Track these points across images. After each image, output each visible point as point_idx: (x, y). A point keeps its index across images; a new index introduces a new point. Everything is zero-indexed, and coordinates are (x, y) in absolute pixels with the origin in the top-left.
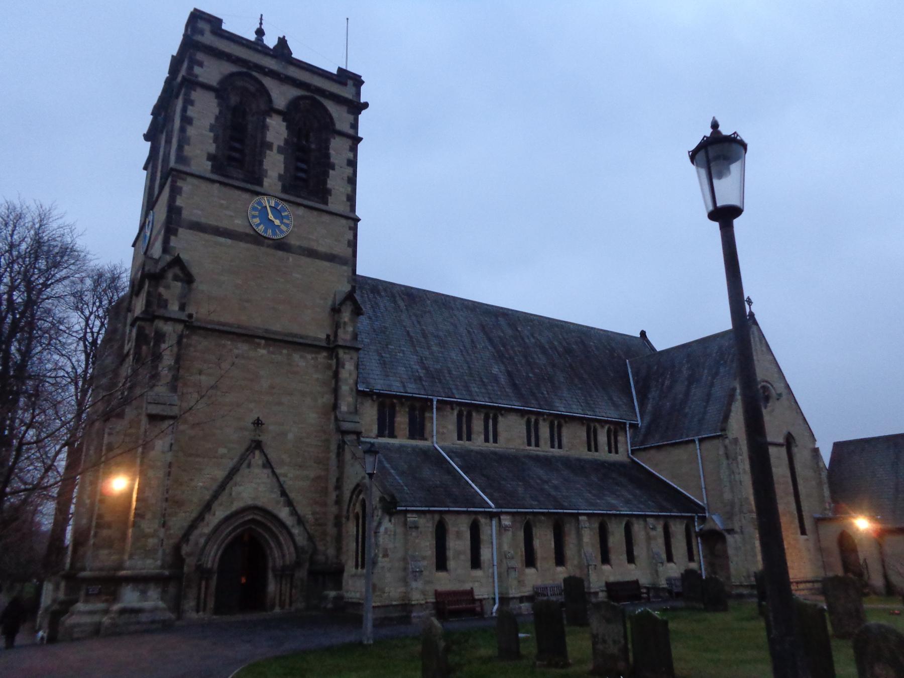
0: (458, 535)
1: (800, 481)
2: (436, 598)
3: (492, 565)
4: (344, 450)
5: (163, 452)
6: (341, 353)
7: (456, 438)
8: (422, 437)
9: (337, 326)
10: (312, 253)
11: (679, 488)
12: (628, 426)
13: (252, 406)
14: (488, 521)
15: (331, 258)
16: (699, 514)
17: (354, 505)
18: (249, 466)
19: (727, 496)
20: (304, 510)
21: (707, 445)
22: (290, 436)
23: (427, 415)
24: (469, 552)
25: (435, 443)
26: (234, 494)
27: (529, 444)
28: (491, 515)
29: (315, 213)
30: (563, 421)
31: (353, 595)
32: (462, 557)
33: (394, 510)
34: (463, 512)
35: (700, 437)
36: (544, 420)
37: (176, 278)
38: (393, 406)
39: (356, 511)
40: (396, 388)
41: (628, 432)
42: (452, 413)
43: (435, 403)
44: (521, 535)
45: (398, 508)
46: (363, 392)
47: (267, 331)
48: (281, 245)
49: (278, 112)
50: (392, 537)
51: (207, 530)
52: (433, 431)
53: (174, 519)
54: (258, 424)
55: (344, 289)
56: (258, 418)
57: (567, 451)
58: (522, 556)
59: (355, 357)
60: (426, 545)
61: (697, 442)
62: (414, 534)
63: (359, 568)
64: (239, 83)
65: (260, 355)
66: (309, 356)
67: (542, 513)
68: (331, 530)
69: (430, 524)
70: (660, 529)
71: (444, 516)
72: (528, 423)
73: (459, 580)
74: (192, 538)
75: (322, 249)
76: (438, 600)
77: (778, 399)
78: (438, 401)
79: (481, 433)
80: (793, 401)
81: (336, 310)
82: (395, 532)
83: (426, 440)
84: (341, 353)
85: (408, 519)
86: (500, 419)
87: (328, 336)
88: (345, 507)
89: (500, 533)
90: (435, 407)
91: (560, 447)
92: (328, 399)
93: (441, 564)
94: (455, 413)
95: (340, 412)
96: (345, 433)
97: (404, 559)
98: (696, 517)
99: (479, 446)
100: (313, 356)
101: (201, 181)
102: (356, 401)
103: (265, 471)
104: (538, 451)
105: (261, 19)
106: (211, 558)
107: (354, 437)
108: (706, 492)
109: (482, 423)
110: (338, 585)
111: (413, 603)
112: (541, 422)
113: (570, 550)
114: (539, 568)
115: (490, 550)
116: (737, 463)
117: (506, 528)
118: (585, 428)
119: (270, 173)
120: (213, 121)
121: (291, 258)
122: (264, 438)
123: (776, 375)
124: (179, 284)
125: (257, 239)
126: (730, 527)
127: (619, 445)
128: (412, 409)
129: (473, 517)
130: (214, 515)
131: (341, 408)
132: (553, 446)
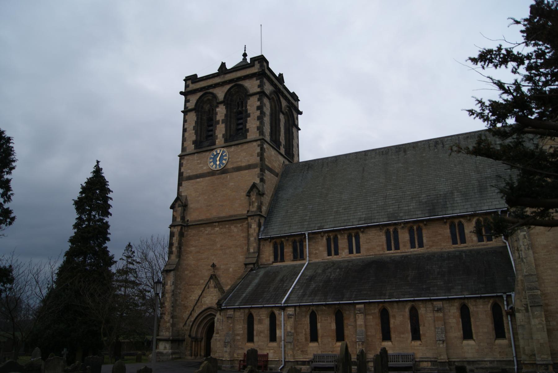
0: (260, 322)
5: (171, 286)
7: (327, 255)
9: (251, 204)
10: (239, 169)
13: (213, 257)
16: (508, 294)
18: (208, 288)
22: (231, 270)
23: (304, 244)
26: (203, 302)
27: (389, 248)
29: (240, 146)
32: (262, 335)
34: (261, 308)
37: (179, 206)
38: (282, 244)
43: (307, 235)
44: (307, 321)
45: (222, 307)
47: (219, 218)
48: (224, 171)
49: (221, 103)
50: (221, 323)
51: (193, 319)
53: (185, 314)
54: (213, 266)
56: (213, 263)
57: (427, 248)
58: (305, 334)
59: (257, 220)
60: (241, 328)
64: (205, 99)
65: (216, 231)
66: (239, 225)
67: (322, 305)
72: (388, 234)
73: (260, 349)
74: (187, 323)
75: (243, 164)
78: (309, 234)
79: (345, 248)
83: (304, 259)
86: (361, 235)
90: (307, 238)
91: (421, 245)
94: (325, 239)
100: (241, 224)
101: (190, 156)
103: (216, 289)
104: (359, 256)
105: (245, 48)
106: (194, 332)
113: (348, 331)
114: (320, 343)
117: (289, 316)
118: (448, 226)
119: (218, 136)
120: (194, 125)
121: (228, 176)
122: (219, 273)
124: (180, 208)
125: (212, 173)
128: (294, 242)
129: (270, 309)
130: (195, 312)
132: (413, 246)
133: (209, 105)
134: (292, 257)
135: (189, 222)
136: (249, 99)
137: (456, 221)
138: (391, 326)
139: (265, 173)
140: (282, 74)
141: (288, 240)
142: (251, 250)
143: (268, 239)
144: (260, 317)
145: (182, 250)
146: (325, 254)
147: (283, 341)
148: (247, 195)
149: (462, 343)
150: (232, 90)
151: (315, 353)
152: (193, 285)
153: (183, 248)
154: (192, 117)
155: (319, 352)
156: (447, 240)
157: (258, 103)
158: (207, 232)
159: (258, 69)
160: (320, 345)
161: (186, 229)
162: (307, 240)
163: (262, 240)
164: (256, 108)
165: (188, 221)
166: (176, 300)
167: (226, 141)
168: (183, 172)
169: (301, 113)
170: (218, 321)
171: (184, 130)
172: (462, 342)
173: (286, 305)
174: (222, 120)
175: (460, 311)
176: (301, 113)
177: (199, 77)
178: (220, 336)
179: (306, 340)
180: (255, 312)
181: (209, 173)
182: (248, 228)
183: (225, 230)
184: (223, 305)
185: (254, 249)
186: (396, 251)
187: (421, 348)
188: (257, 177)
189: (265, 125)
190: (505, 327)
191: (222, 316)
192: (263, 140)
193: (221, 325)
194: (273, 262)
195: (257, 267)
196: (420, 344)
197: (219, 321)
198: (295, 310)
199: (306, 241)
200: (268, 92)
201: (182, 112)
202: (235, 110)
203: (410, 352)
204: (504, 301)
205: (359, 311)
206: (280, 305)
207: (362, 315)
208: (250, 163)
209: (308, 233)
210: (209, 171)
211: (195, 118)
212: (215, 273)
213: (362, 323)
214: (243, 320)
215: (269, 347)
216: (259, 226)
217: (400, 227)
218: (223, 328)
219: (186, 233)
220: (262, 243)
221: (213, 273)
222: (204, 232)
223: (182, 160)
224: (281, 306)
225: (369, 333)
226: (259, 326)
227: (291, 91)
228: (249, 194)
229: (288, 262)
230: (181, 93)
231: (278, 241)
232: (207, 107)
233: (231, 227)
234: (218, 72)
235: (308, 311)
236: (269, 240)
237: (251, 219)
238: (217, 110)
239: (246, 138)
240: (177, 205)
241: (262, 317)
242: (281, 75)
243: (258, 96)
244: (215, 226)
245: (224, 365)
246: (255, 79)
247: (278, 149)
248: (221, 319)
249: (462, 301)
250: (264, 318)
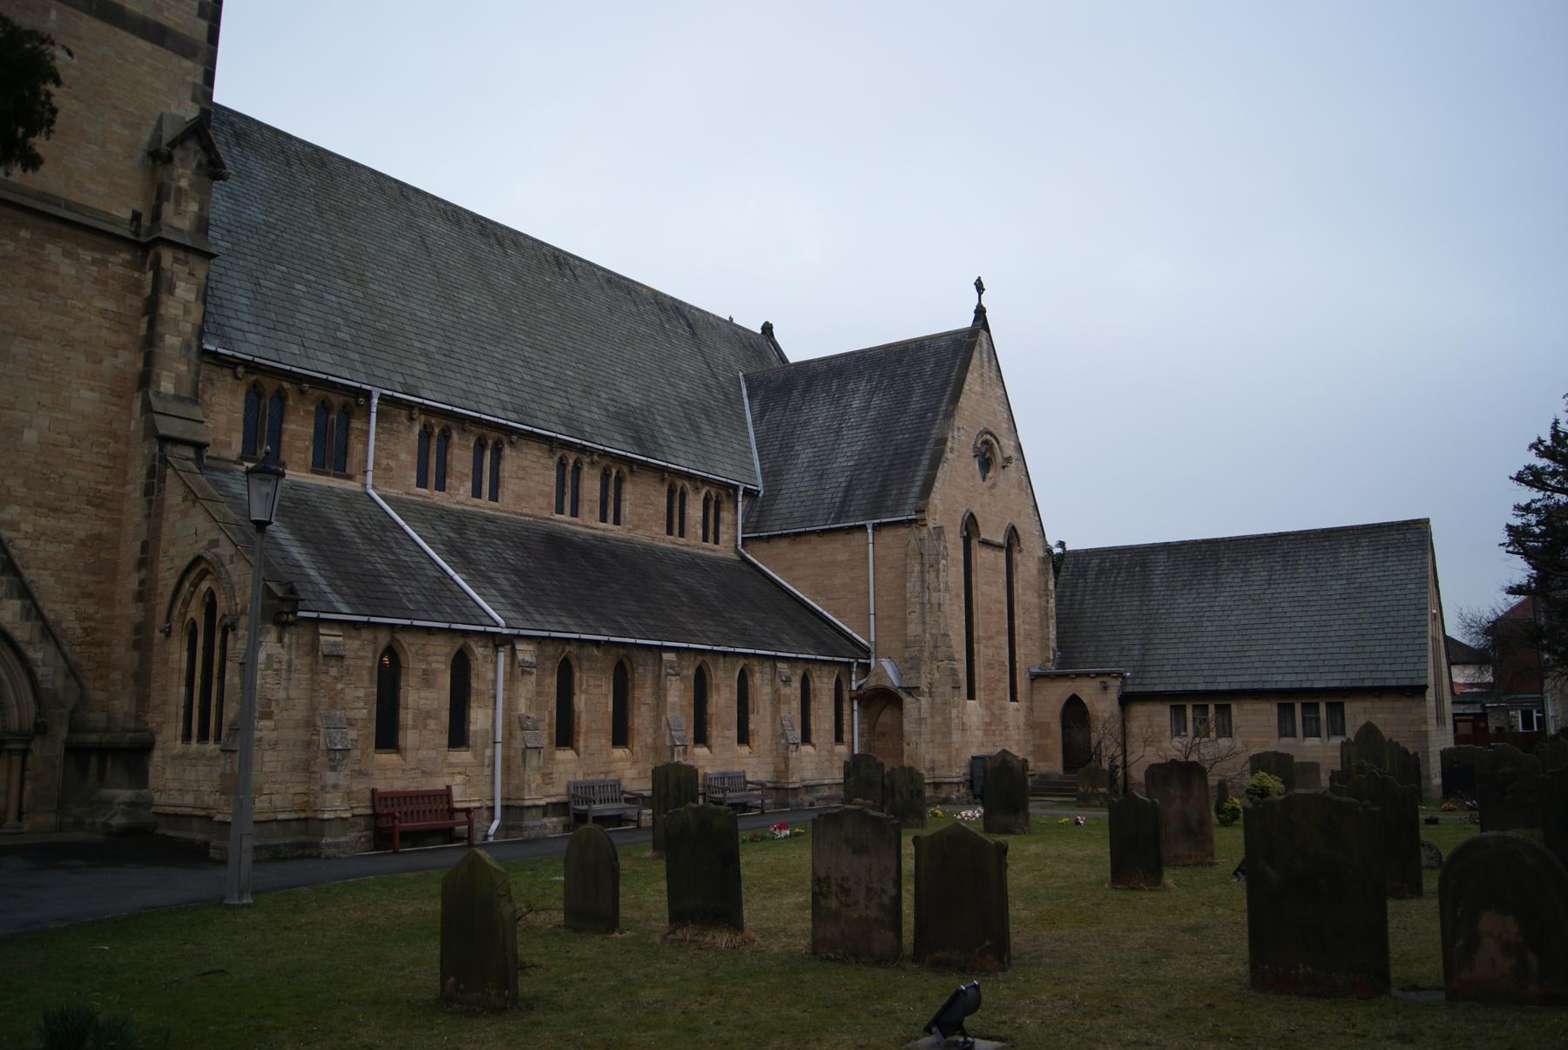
0: (427, 679)
1: (1018, 610)
2: (373, 807)
3: (490, 742)
4: (163, 479)
6: (167, 257)
7: (414, 480)
8: (342, 472)
9: (161, 193)
11: (825, 613)
12: (741, 493)
14: (489, 652)
15: (157, 34)
16: (860, 661)
17: (186, 603)
19: (913, 629)
20: (62, 609)
21: (887, 536)
22: (30, 436)
23: (356, 424)
24: (445, 715)
25: (369, 486)
28: (498, 641)
30: (625, 469)
31: (176, 798)
32: (432, 724)
33: (291, 617)
35: (878, 521)
36: (592, 463)
38: (281, 397)
39: (188, 618)
40: (292, 358)
41: (740, 505)
42: (410, 428)
43: (375, 401)
44: (551, 684)
45: (301, 614)
46: (215, 354)
50: (284, 675)
52: (366, 461)
55: (181, 113)
57: (630, 529)
58: (550, 725)
59: (201, 273)
60: (359, 699)
61: (870, 531)
62: (334, 672)
63: (194, 740)
66: (87, 256)
67: (597, 643)
68: (122, 653)
69: (368, 653)
70: (796, 684)
71: (398, 636)
72: (562, 465)
73: (423, 772)
76: (379, 810)
77: (1004, 467)
78: (382, 398)
79: (466, 475)
80: (1024, 473)
81: (159, 157)
83: (350, 477)
84: (167, 257)
85: (322, 638)
86: (507, 451)
87: (136, 216)
88: (162, 608)
89: (511, 679)
90: (374, 409)
92: (128, 361)
93: (387, 735)
94: (417, 429)
95: (158, 393)
96: (164, 440)
97: (310, 724)
98: (855, 664)
99: (461, 503)
100: (98, 256)
102: (197, 374)
107: (190, 453)
108: (875, 620)
109: (470, 454)
110: (139, 776)
111: (326, 816)
112: (585, 469)
113: (641, 719)
114: (582, 749)
115: (490, 712)
116: (938, 571)
117: (526, 669)
123: (1005, 425)
126: (913, 683)
127: (722, 528)
128: (324, 408)
129: (460, 642)
131: (159, 386)
132: (603, 519)
141: (302, 392)
144: (430, 665)
151: (571, 779)
155: (580, 778)
160: (582, 756)
162: (374, 416)
170: (268, 666)
178: (276, 729)
179: (550, 743)
180: (410, 644)
183: (11, 247)
185: (178, 382)
187: (751, 759)
190: (844, 722)
191: (290, 647)
193: (284, 683)
197: (276, 666)
203: (737, 769)
204: (851, 674)
205: (672, 668)
208: (160, 19)
209: (382, 394)
214: (372, 668)
215: (451, 765)
218: (293, 694)
226: (423, 694)
231: (269, 385)
233: (43, 248)
237: (176, 260)
241: (435, 665)
245: (329, 840)
248: (285, 658)
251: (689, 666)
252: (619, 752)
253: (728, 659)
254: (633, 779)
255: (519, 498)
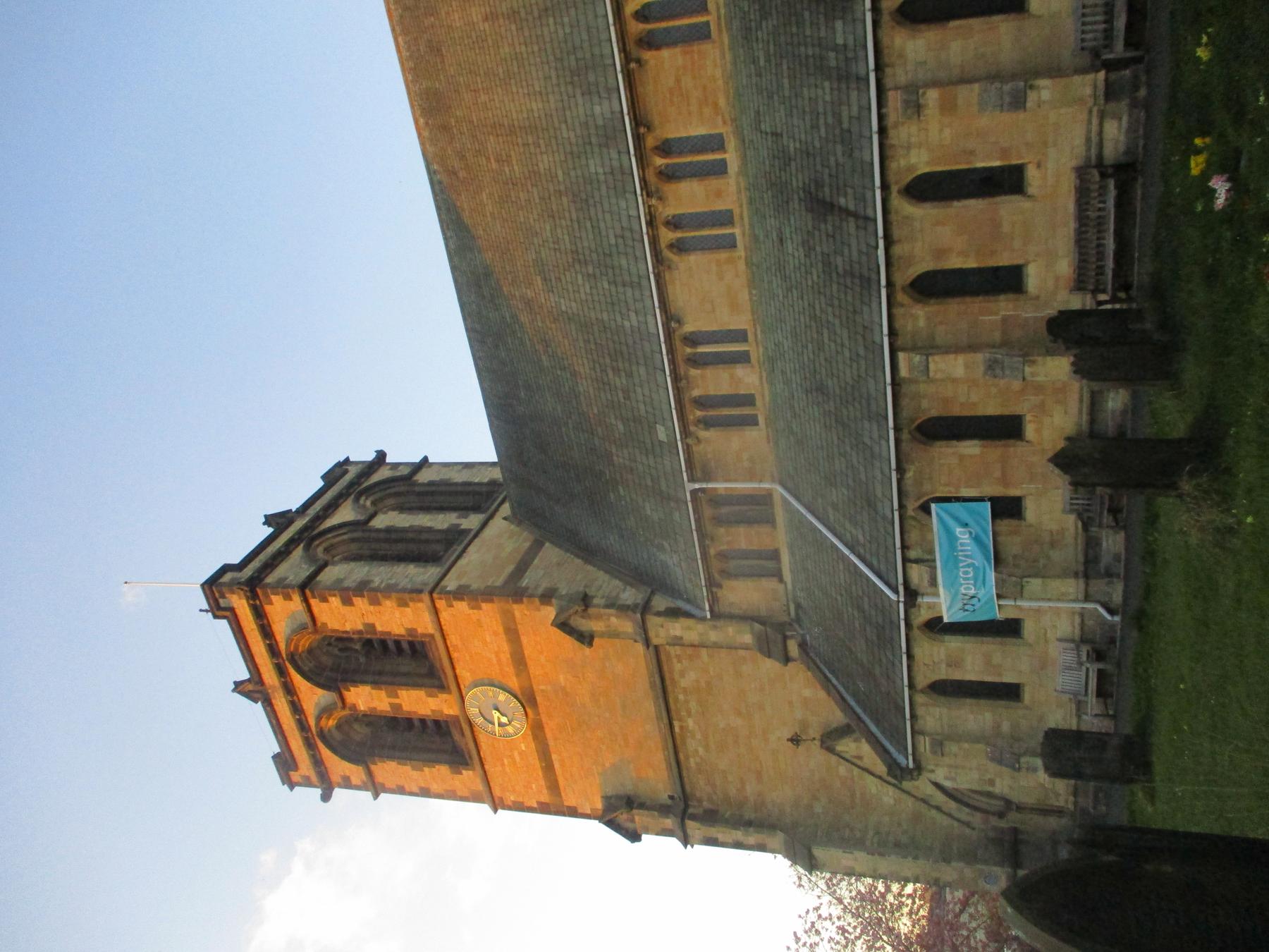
0: (954, 663)
5: (856, 860)
10: (519, 661)
18: (860, 758)
27: (730, 244)
29: (455, 655)
32: (997, 659)
34: (910, 656)
37: (633, 821)
38: (723, 556)
45: (911, 765)
47: (659, 718)
48: (528, 699)
56: (788, 740)
59: (659, 620)
66: (678, 667)
67: (899, 481)
72: (680, 247)
74: (963, 817)
75: (505, 647)
79: (732, 376)
82: (950, 766)
86: (689, 328)
94: (703, 434)
99: (761, 378)
100: (675, 660)
101: (492, 784)
118: (648, 55)
121: (540, 687)
124: (637, 818)
125: (537, 729)
128: (718, 521)
129: (916, 633)
131: (747, 644)
132: (719, 169)
133: (356, 726)
134: (765, 529)
135: (676, 796)
136: (325, 624)
137: (636, 28)
138: (971, 264)
139: (527, 588)
140: (266, 516)
142: (746, 641)
143: (712, 592)
144: (942, 660)
145: (753, 816)
146: (751, 434)
147: (1019, 603)
148: (590, 644)
149: (1040, 17)
150: (306, 669)
152: (853, 796)
153: (749, 815)
154: (386, 770)
156: (696, 56)
157: (335, 601)
158: (701, 750)
159: (240, 599)
161: (695, 803)
162: (710, 485)
163: (716, 609)
164: (348, 608)
165: (671, 797)
166: (897, 845)
167: (442, 687)
168: (538, 803)
169: (381, 456)
170: (953, 779)
171: (425, 793)
172: (1034, 16)
173: (901, 589)
174: (389, 696)
175: (923, 27)
176: (381, 456)
177: (277, 749)
181: (535, 737)
182: (683, 645)
184: (901, 759)
186: (736, 218)
188: (537, 612)
189: (393, 581)
192: (435, 589)
194: (781, 580)
195: (796, 626)
196: (1039, 166)
198: (917, 561)
199: (715, 489)
200: (306, 571)
201: (376, 796)
202: (362, 660)
206: (901, 606)
207: (934, 361)
208: (501, 630)
209: (689, 481)
210: (530, 738)
211: (392, 765)
212: (818, 737)
213: (961, 359)
216: (674, 613)
217: (660, 209)
219: (705, 803)
220: (723, 608)
221: (817, 743)
222: (701, 758)
223: (506, 803)
224: (905, 603)
225: (997, 336)
227: (321, 484)
228: (585, 638)
229: (781, 538)
230: (326, 797)
232: (361, 732)
233: (684, 688)
234: (260, 703)
235: (919, 522)
236: (714, 590)
237: (657, 636)
238: (362, 709)
239: (432, 636)
240: (629, 825)
241: (943, 657)
242: (269, 520)
243: (313, 602)
244: (681, 728)
246: (268, 608)
247: (472, 533)
249: (886, 18)
250: (942, 650)
251: (912, 315)
252: (1030, 431)
253: (896, 233)
254: (1066, 413)
255: (734, 307)
